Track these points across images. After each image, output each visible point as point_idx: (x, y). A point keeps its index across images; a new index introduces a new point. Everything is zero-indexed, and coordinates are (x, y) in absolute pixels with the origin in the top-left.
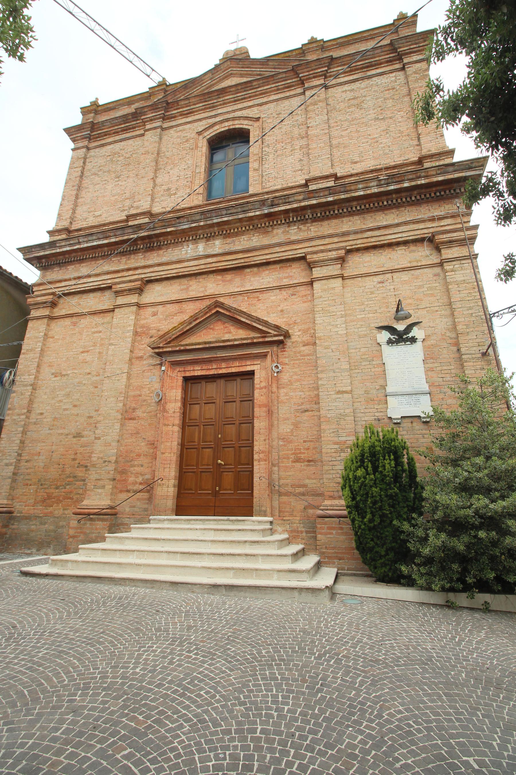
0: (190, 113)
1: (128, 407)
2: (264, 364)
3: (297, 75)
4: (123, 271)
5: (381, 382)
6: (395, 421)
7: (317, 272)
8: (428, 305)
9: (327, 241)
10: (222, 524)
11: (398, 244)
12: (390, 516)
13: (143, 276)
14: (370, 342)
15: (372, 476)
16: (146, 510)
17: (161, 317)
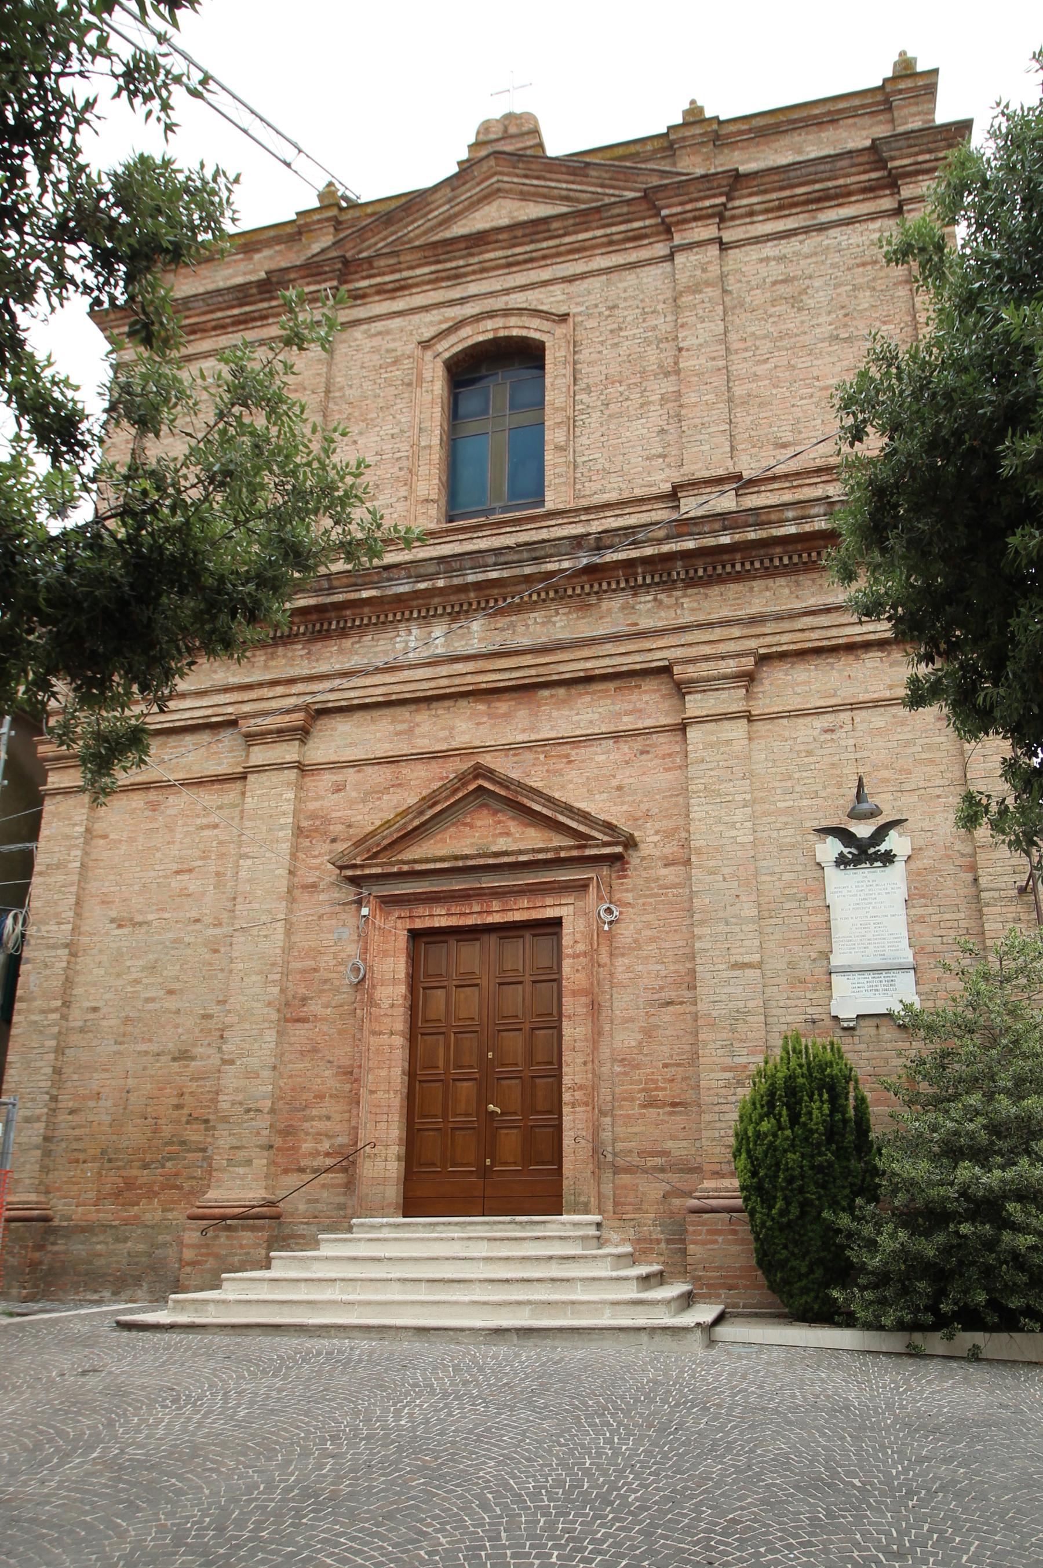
0: (401, 288)
1: (290, 994)
4: (261, 685)
5: (820, 944)
6: (845, 1025)
7: (696, 705)
8: (921, 784)
9: (717, 633)
13: (309, 699)
14: (801, 860)
16: (342, 1207)
17: (354, 794)
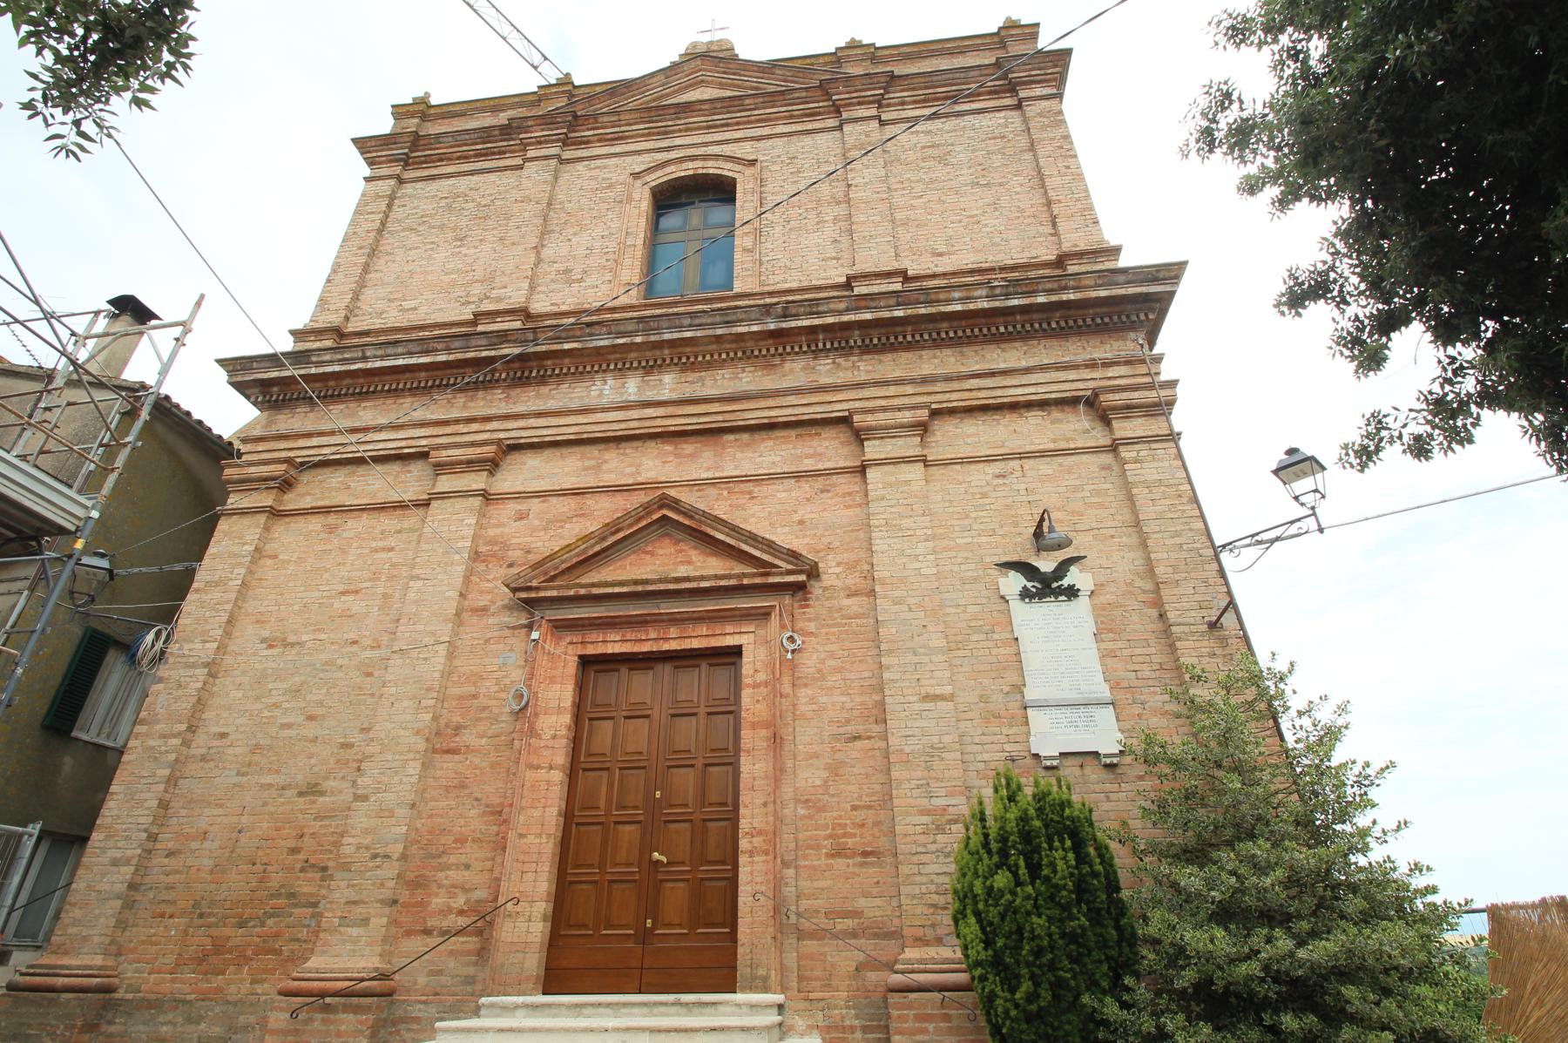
0: (619, 138)
1: (443, 722)
2: (762, 632)
3: (828, 96)
4: (457, 421)
5: (1013, 678)
6: (1048, 763)
7: (873, 449)
8: (1094, 525)
9: (892, 390)
10: (663, 1015)
11: (1029, 405)
12: (1072, 983)
13: (502, 435)
14: (985, 592)
15: (1029, 889)
16: (470, 980)
17: (536, 522)
